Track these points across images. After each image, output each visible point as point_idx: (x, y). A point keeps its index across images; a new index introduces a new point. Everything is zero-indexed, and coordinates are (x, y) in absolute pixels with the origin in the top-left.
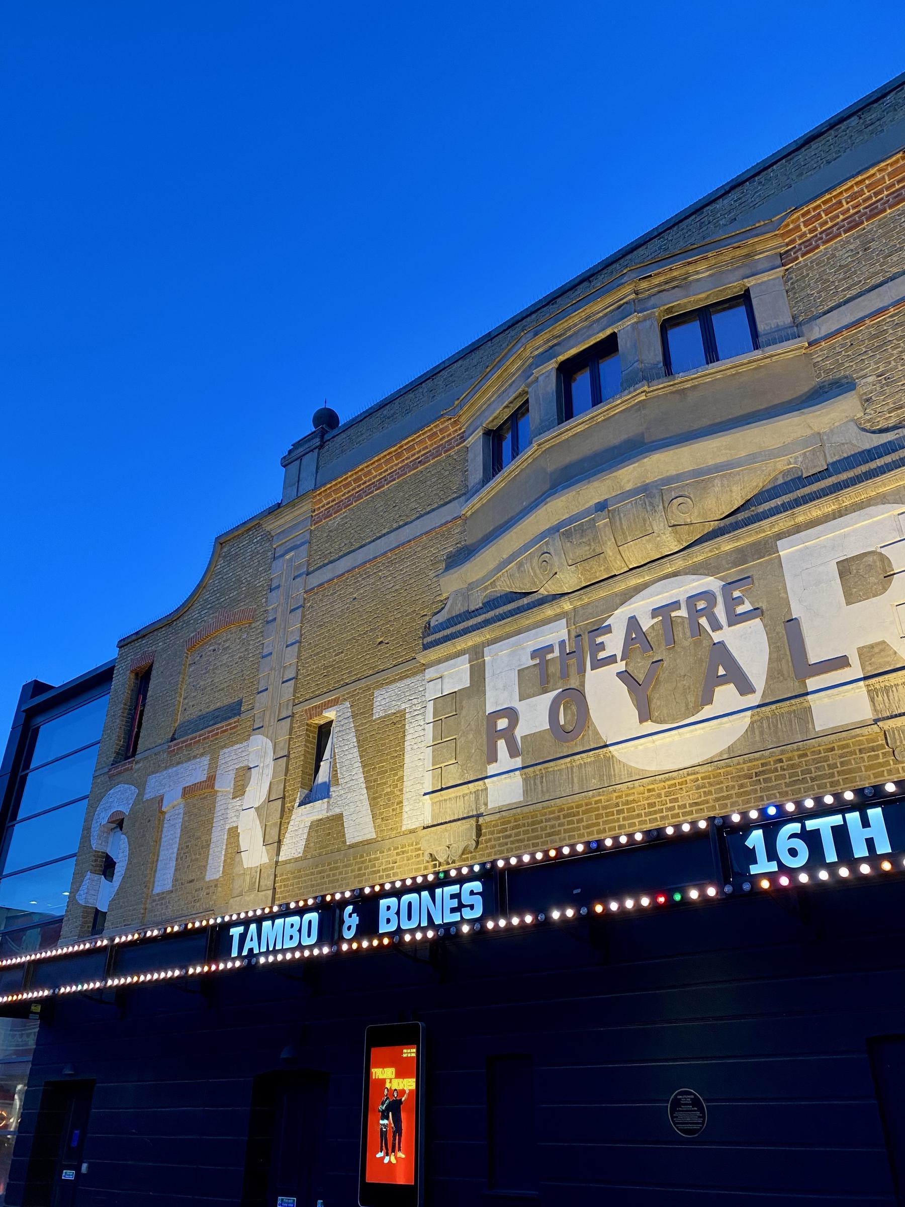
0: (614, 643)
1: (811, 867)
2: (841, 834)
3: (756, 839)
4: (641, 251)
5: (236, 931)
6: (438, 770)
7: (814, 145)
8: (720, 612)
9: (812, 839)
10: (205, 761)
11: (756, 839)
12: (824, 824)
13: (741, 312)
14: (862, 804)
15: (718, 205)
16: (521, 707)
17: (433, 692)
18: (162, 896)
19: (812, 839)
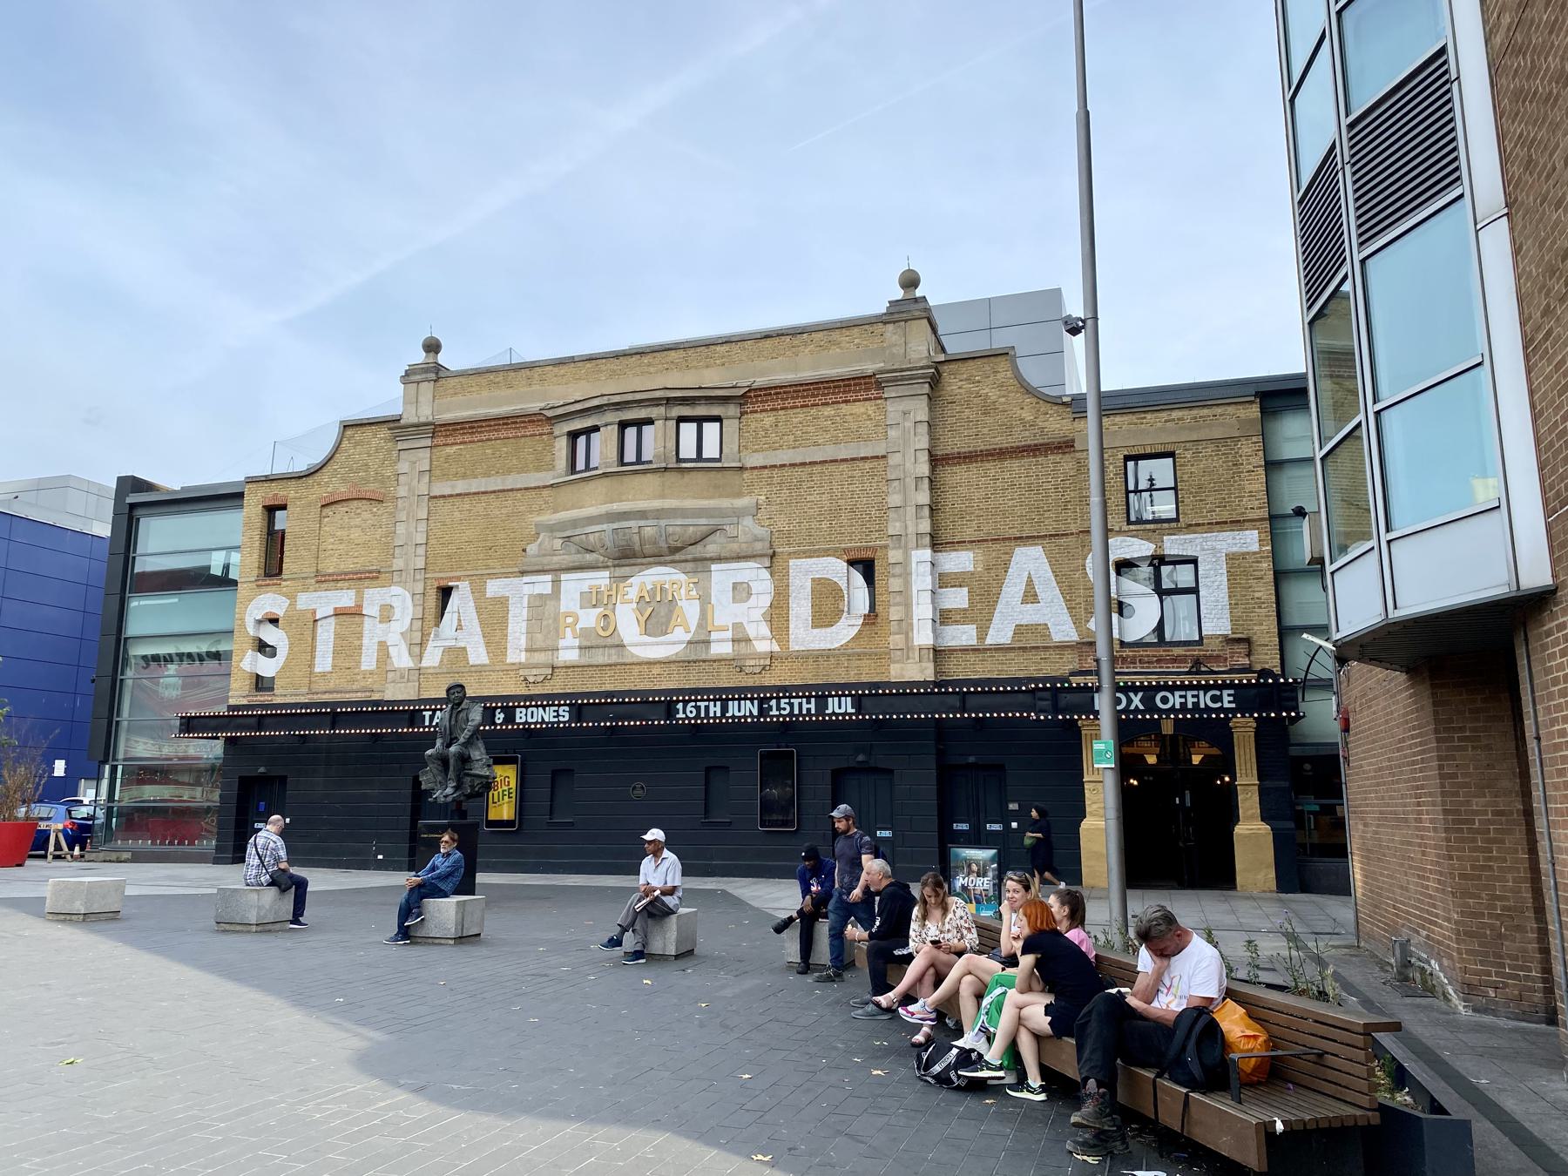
0: (633, 594)
1: (695, 718)
2: (707, 708)
3: (680, 706)
4: (673, 353)
5: (427, 714)
6: (530, 639)
7: (769, 341)
8: (683, 591)
9: (698, 708)
10: (352, 593)
11: (680, 706)
12: (702, 704)
13: (717, 425)
14: (715, 700)
15: (718, 348)
16: (581, 613)
17: (527, 590)
18: (324, 674)
19: (698, 708)
